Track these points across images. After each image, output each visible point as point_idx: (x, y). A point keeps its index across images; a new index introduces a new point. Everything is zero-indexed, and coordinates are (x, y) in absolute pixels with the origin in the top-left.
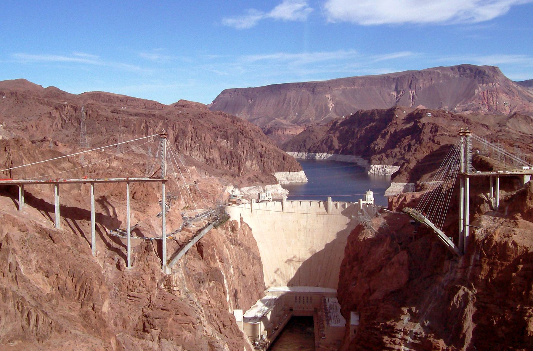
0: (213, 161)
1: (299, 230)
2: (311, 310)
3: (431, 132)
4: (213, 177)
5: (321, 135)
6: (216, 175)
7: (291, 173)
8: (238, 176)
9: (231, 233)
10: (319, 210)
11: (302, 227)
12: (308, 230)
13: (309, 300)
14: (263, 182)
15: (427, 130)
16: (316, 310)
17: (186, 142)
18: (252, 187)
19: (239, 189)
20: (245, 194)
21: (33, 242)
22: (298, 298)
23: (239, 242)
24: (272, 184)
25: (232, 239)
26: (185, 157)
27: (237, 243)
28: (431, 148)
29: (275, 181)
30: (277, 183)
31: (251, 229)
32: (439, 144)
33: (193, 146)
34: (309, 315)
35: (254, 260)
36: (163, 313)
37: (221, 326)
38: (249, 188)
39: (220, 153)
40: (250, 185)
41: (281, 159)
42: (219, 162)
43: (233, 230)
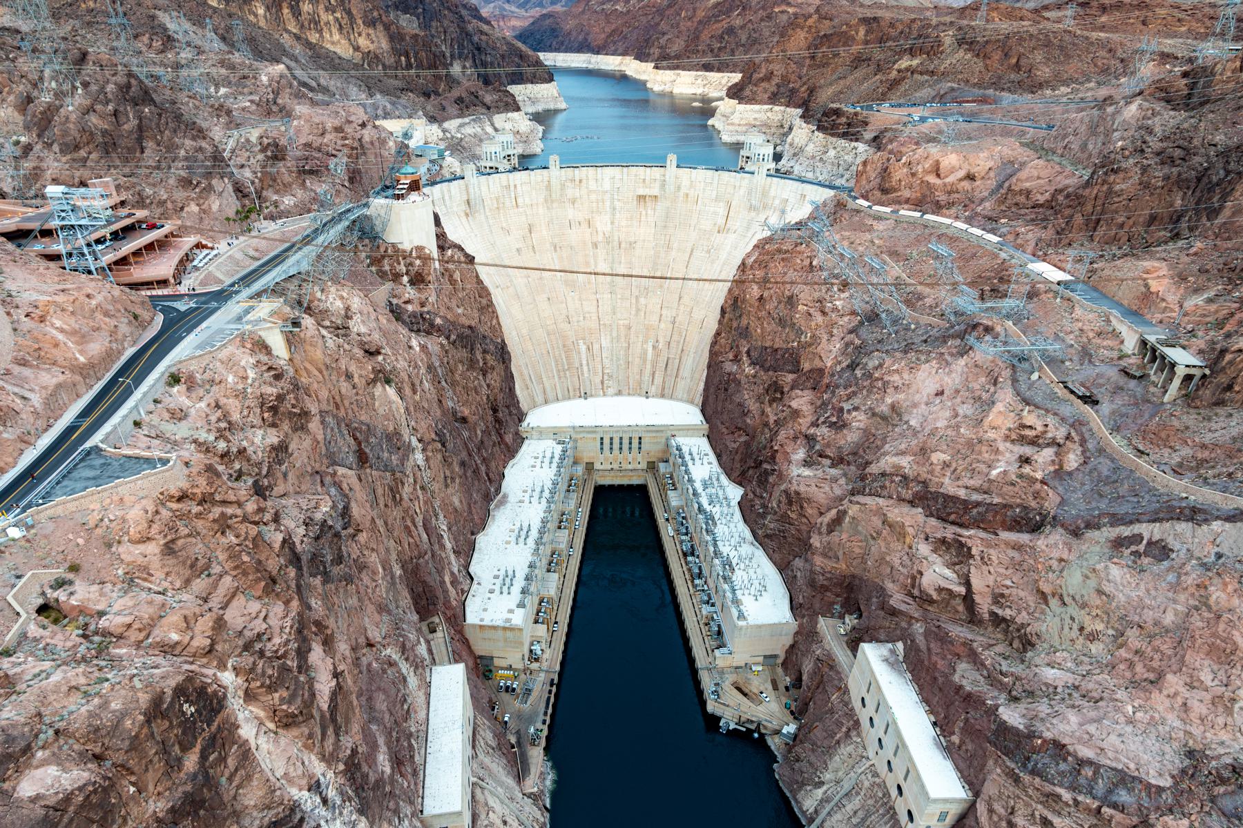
0: (377, 57)
1: (595, 245)
2: (639, 467)
4: (378, 96)
6: (385, 92)
8: (437, 94)
9: (410, 292)
11: (600, 238)
12: (616, 244)
14: (489, 108)
16: (652, 466)
18: (467, 120)
19: (440, 126)
22: (607, 441)
23: (438, 321)
24: (507, 111)
25: (414, 315)
26: (309, 45)
27: (432, 325)
29: (512, 105)
30: (518, 109)
31: (471, 260)
34: (636, 481)
35: (488, 357)
38: (459, 121)
39: (391, 38)
40: (461, 116)
42: (390, 61)
43: (418, 280)
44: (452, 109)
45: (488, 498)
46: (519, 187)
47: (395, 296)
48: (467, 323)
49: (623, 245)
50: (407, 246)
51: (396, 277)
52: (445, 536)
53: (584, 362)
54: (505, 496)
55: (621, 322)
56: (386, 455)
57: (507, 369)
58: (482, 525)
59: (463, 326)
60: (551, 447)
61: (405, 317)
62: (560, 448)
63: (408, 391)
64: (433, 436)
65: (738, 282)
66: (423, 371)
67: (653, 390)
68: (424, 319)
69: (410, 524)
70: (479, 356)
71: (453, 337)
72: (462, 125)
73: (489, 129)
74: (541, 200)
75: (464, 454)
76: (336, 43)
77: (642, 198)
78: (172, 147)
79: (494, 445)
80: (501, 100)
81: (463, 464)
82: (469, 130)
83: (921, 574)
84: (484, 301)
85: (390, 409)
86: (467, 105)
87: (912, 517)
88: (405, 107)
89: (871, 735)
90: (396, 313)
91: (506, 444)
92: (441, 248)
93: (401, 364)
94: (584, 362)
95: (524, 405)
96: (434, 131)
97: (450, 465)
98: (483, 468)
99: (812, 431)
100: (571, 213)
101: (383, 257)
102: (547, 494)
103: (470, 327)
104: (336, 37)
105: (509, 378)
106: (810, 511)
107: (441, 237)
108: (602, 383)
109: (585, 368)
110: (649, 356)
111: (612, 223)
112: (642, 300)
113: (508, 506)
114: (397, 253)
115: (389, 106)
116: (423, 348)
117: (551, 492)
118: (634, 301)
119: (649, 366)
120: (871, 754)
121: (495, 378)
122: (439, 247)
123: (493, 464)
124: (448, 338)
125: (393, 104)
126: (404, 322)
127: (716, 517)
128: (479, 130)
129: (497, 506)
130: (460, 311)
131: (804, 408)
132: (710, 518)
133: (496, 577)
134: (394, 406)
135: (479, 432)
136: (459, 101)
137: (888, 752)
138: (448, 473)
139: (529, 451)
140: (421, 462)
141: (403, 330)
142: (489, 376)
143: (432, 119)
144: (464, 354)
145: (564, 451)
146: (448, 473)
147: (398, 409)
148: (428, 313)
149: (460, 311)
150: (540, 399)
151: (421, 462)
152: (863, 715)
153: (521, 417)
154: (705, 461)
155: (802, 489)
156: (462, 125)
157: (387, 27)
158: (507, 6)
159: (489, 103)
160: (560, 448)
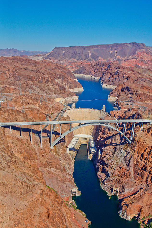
1: (83, 117)
4: (57, 95)
5: (87, 69)
6: (58, 94)
7: (79, 88)
8: (64, 94)
13: (86, 139)
15: (121, 74)
17: (48, 83)
18: (68, 98)
21: (16, 143)
26: (48, 88)
33: (50, 85)
36: (51, 161)
37: (65, 158)
38: (67, 98)
40: (68, 97)
41: (76, 84)
42: (58, 89)
44: (66, 96)
50: (65, 117)
72: (67, 98)
73: (71, 99)
76: (52, 88)
78: (48, 108)
80: (73, 94)
82: (68, 99)
92: (67, 117)
95: (74, 134)
96: (63, 100)
100: (81, 113)
104: (52, 86)
107: (67, 116)
114: (63, 117)
125: (59, 96)
143: (64, 98)
150: (76, 134)
156: (67, 98)
157: (58, 85)
158: (74, 60)
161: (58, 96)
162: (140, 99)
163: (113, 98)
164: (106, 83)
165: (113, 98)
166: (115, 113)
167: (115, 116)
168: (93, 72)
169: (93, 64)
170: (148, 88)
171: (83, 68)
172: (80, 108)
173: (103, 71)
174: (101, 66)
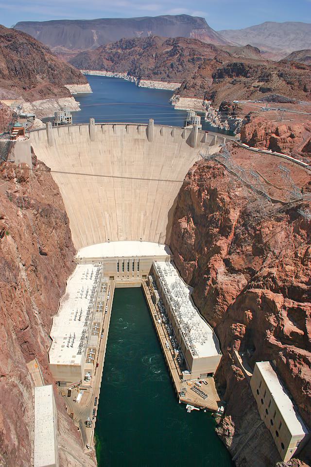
1: (112, 163)
3: (190, 55)
7: (79, 86)
9: (18, 187)
10: (137, 136)
11: (116, 159)
14: (56, 95)
15: (186, 53)
18: (45, 101)
19: (31, 103)
20: (37, 109)
22: (121, 265)
23: (33, 202)
24: (66, 97)
25: (20, 198)
27: (29, 203)
28: (214, 66)
31: (49, 170)
32: (222, 63)
38: (41, 101)
39: (7, 62)
41: (70, 73)
42: (6, 72)
43: (22, 180)
45: (59, 296)
46: (74, 134)
47: (9, 189)
48: (47, 203)
49: (127, 163)
51: (11, 178)
52: (37, 317)
53: (108, 223)
54: (68, 295)
55: (127, 202)
56: (7, 273)
57: (68, 227)
58: (56, 312)
59: (45, 204)
60: (91, 268)
61: (15, 200)
62: (96, 269)
63: (17, 238)
64: (31, 263)
65: (186, 184)
66: (25, 228)
67: (144, 238)
68: (25, 201)
69: (19, 310)
70: (53, 220)
71: (40, 210)
73: (56, 105)
74: (85, 139)
75: (46, 273)
77: (136, 140)
79: (61, 267)
81: (45, 278)
82: (46, 106)
83: (283, 326)
84: (55, 192)
85: (9, 248)
86: (44, 94)
87: (279, 299)
88: (13, 94)
89: (262, 408)
90: (11, 197)
91: (68, 267)
92: (35, 165)
93: (14, 225)
94: (108, 223)
95: (76, 246)
97: (39, 278)
98: (56, 280)
99: (227, 257)
101: (4, 169)
102: (90, 293)
103: (49, 205)
105: (69, 231)
106: (228, 297)
107: (34, 158)
108: (118, 234)
109: (108, 226)
110: (142, 220)
111: (122, 152)
112: (138, 191)
113: (70, 300)
115: (5, 94)
116: (25, 215)
117: (92, 292)
118: (133, 191)
119: (142, 225)
120: (262, 417)
121: (61, 233)
122: (33, 164)
123: (61, 278)
124: (38, 211)
126: (14, 202)
127: (181, 303)
128: (51, 105)
129: (64, 301)
130: (43, 196)
131: (223, 245)
132: (177, 304)
133: (65, 338)
134: (11, 246)
135: (53, 260)
136: (41, 92)
137: (270, 417)
138: (38, 283)
139: (80, 270)
140: (24, 277)
141: (15, 207)
142: (58, 230)
143: (27, 100)
144: (45, 220)
145: (98, 270)
146: (38, 283)
147: (13, 248)
148: (27, 197)
149: (43, 196)
151: (24, 277)
152: (258, 399)
153: (75, 252)
154: (173, 275)
155: (224, 286)
156: (42, 103)
158: (63, 48)
159: (56, 93)
160: (96, 269)
161: (5, 94)
162: (303, 92)
163: (189, 101)
164: (149, 77)
165: (190, 101)
166: (277, 133)
167: (280, 145)
168: (106, 63)
169: (108, 47)
170: (302, 66)
171: (84, 56)
172: (92, 120)
173: (132, 58)
174: (126, 48)
